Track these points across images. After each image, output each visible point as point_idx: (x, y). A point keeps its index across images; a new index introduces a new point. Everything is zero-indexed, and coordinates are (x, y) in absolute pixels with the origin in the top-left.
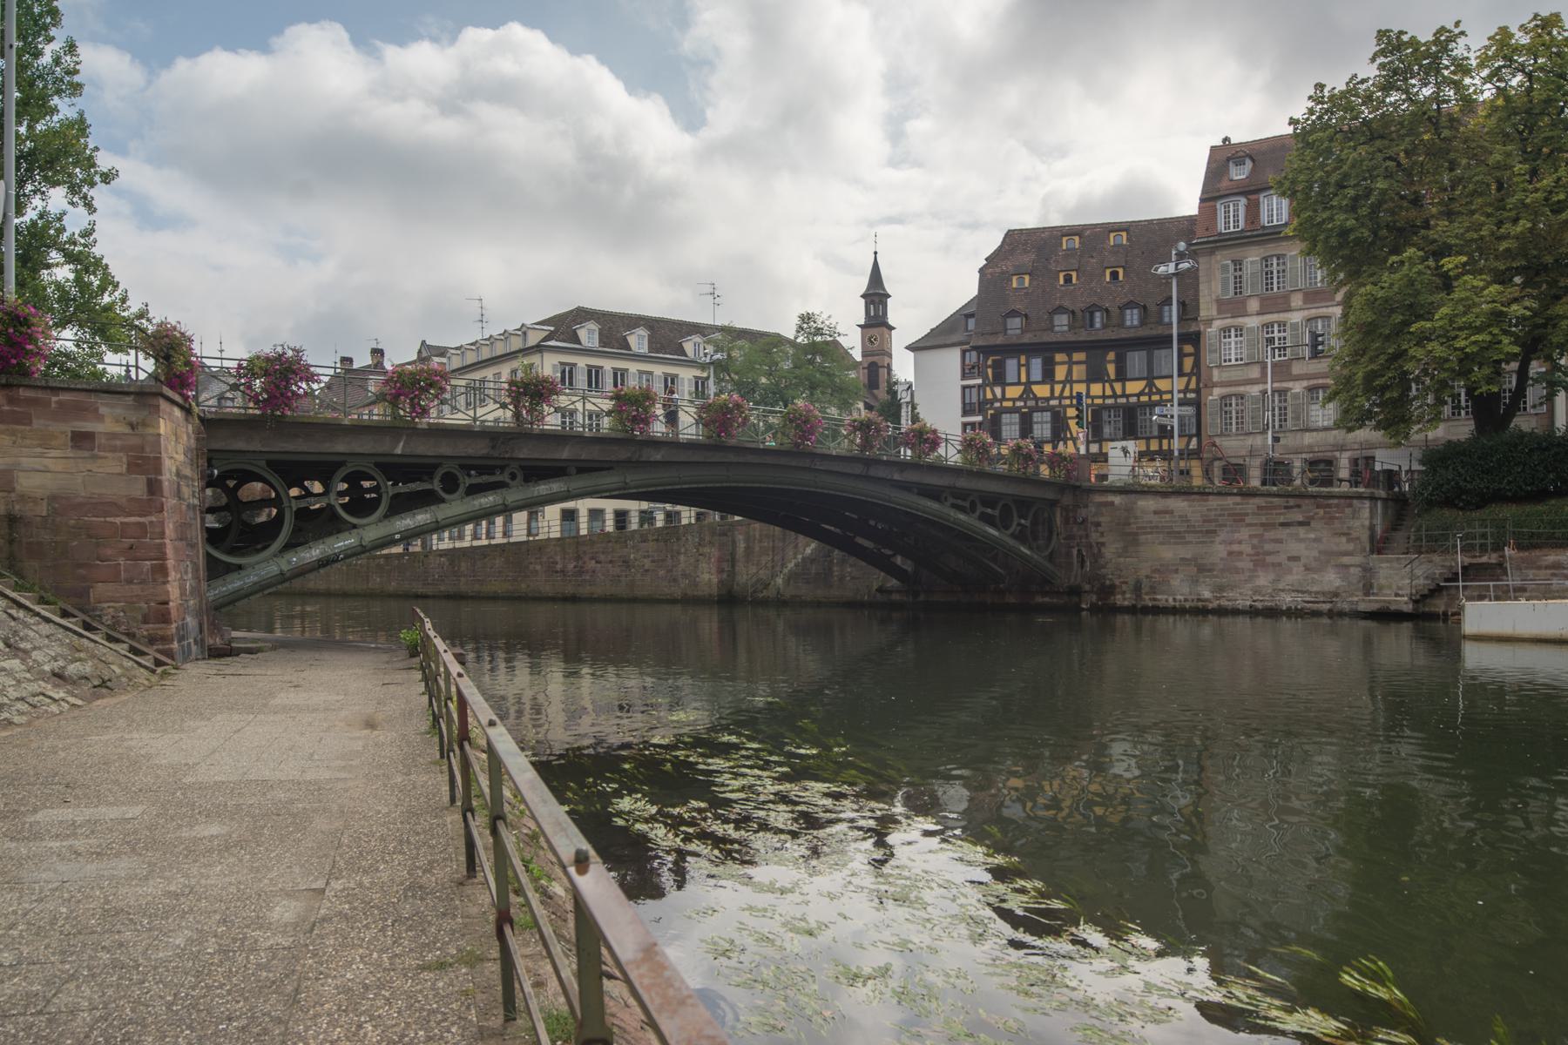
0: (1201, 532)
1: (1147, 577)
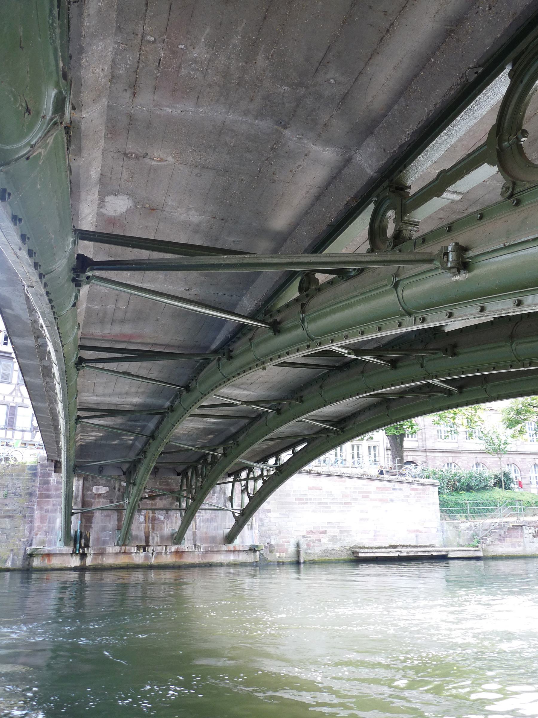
0: (341, 503)
1: (304, 537)
